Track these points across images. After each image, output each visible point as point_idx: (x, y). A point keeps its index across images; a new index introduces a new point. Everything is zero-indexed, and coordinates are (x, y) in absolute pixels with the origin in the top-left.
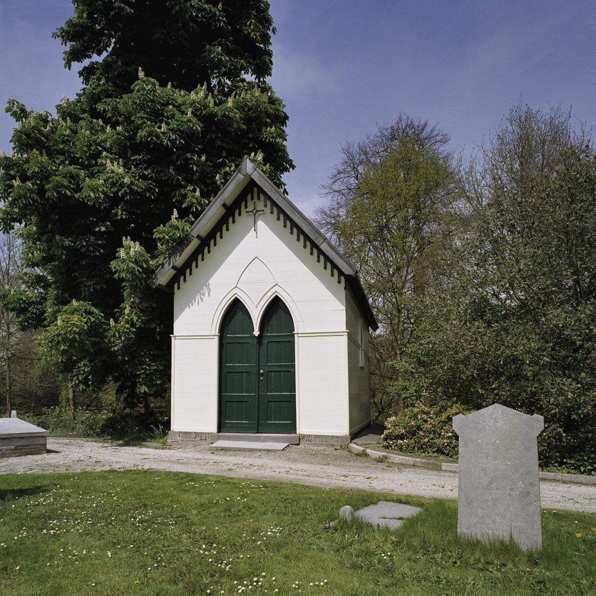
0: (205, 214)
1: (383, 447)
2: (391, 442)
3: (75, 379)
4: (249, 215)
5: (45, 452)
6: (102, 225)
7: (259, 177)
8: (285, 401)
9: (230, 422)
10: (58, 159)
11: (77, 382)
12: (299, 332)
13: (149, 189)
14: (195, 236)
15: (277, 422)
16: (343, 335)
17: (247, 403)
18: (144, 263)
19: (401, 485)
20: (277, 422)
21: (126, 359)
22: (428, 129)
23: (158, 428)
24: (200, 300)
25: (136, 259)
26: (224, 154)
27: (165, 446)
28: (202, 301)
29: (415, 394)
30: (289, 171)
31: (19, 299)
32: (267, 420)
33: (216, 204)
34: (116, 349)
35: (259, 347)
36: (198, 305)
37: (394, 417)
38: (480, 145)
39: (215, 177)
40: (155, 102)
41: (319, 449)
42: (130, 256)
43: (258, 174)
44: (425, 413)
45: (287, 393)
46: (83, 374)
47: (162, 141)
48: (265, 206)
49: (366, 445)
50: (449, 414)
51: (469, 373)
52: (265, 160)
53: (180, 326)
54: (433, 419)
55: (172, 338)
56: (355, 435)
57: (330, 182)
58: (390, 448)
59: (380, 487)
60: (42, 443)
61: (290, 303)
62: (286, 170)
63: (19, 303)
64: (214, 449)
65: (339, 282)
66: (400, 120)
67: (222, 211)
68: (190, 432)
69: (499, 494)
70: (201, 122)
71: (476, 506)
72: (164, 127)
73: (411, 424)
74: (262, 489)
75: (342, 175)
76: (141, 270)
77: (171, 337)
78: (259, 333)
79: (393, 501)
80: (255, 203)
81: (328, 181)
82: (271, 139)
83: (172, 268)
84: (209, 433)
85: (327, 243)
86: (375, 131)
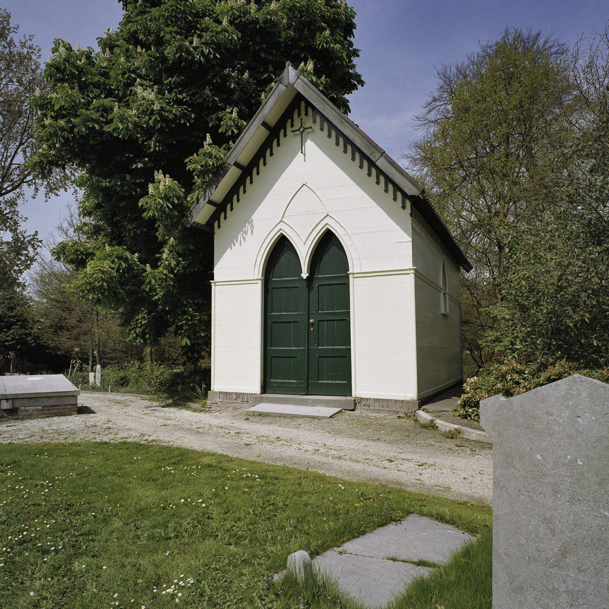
0: (243, 136)
1: (459, 416)
2: (470, 410)
3: (132, 332)
4: (295, 135)
5: (76, 413)
6: (139, 162)
7: (303, 86)
8: (339, 357)
9: (275, 381)
10: (92, 92)
11: (135, 335)
12: (354, 272)
13: (184, 116)
14: (232, 164)
15: (330, 382)
16: (409, 274)
17: (296, 359)
18: (175, 198)
19: (465, 478)
20: (330, 382)
21: (167, 309)
22: (541, 42)
23: (201, 388)
24: (242, 239)
25: (165, 195)
26: (271, 69)
27: (204, 409)
28: (245, 241)
29: (511, 347)
30: (357, 89)
31: (77, 251)
32: (318, 380)
33: (255, 123)
34: (156, 297)
35: (309, 292)
36: (240, 245)
37: (475, 377)
38: (603, 32)
39: (260, 96)
40: (186, 13)
41: (378, 415)
42: (159, 192)
43: (301, 82)
44: (517, 372)
45: (342, 347)
46: (141, 327)
47: (193, 57)
48: (314, 122)
49: (439, 414)
50: (549, 374)
51: (576, 317)
52: (317, 72)
53: (220, 271)
54: (528, 380)
55: (212, 284)
56: (424, 401)
57: (425, 111)
58: (469, 418)
59: (432, 481)
60: (72, 403)
61: (344, 237)
62: (354, 87)
63: (77, 255)
64: (250, 414)
65: (404, 207)
66: (507, 35)
67: (263, 133)
68: (231, 393)
69: (584, 582)
70: (240, 31)
71: (530, 599)
72: (196, 41)
73: (497, 387)
74: (258, 480)
75: (438, 103)
76: (171, 207)
77: (211, 283)
78: (307, 275)
79: (431, 516)
80: (302, 119)
81: (421, 112)
82: (325, 45)
83: (207, 203)
84: (251, 394)
85: (384, 157)
86: (478, 50)
